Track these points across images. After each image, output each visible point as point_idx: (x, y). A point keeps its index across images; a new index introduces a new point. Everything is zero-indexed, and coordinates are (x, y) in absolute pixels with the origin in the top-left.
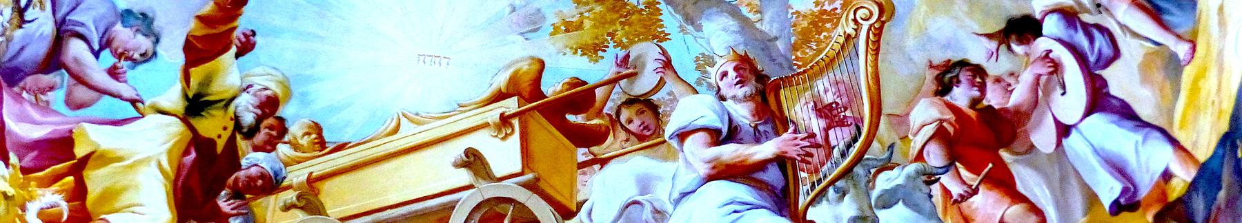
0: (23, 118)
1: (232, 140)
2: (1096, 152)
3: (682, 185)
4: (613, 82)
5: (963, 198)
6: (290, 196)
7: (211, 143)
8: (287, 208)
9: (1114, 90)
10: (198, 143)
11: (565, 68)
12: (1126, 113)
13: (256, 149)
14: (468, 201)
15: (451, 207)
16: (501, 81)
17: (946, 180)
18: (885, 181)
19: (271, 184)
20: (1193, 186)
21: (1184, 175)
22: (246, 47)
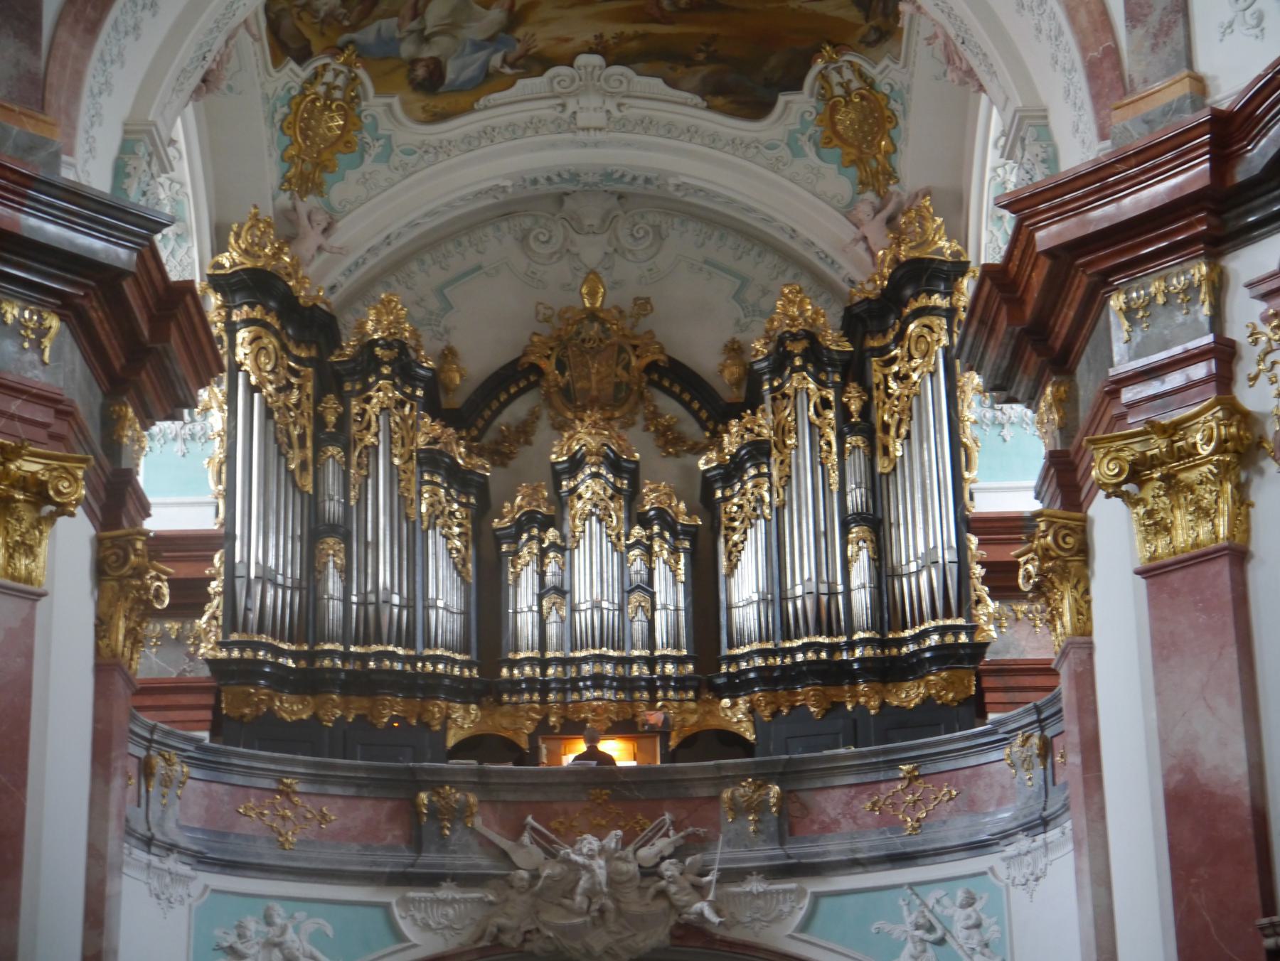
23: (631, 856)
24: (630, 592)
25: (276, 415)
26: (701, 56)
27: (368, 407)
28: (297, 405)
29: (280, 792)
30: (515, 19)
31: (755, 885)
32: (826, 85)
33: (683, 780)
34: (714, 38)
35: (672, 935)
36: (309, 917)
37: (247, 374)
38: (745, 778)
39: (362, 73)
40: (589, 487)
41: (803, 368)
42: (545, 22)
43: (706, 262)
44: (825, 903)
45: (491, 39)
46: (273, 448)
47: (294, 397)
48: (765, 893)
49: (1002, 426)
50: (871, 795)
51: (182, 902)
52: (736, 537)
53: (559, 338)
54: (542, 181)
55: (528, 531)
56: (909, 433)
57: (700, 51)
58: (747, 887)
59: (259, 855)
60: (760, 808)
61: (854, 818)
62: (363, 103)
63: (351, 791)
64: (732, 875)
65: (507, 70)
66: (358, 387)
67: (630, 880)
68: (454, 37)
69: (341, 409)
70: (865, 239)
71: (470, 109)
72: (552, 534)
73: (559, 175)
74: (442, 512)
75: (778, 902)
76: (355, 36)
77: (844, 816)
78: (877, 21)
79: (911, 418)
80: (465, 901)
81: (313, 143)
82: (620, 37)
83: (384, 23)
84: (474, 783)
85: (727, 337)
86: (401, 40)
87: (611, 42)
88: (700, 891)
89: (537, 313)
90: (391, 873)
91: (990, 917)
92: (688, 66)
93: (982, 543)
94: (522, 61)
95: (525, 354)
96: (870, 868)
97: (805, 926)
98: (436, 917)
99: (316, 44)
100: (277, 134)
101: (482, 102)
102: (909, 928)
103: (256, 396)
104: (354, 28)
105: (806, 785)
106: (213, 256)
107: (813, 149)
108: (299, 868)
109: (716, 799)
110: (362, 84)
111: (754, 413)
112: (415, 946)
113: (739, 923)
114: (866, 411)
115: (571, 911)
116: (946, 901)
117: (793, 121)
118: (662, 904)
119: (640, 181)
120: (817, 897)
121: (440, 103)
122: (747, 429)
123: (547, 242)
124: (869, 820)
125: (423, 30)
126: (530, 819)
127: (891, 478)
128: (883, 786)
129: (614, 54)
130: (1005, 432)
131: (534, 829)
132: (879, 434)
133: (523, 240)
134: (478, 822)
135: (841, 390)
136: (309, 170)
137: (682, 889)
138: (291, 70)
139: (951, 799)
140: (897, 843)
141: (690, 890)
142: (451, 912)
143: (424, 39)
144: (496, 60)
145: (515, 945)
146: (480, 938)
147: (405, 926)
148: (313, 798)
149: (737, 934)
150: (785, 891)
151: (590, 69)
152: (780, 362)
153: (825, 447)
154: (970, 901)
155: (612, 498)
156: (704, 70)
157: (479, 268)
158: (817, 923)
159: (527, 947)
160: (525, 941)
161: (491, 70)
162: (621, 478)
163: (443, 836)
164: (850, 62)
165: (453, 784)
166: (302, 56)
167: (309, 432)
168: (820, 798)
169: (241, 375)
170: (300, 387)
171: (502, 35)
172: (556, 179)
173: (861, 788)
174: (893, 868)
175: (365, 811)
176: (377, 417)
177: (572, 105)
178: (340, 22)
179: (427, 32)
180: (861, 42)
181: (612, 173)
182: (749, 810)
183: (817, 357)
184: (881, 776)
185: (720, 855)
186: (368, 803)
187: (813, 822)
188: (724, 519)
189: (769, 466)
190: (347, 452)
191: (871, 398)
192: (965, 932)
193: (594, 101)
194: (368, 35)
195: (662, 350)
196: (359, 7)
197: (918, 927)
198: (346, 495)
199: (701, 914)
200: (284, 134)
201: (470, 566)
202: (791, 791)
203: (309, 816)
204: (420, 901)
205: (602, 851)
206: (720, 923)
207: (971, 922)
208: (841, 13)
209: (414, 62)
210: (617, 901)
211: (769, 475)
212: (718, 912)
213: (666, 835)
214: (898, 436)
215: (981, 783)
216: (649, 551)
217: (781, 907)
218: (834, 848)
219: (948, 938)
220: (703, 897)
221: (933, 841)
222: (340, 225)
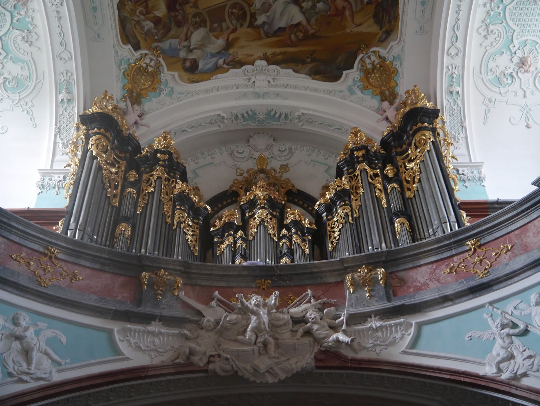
24: (281, 257)
25: (104, 172)
26: (309, 60)
27: (151, 178)
28: (117, 173)
29: (46, 255)
30: (229, 45)
31: (375, 323)
32: (363, 64)
33: (317, 273)
34: (314, 51)
35: (316, 359)
36: (48, 328)
37: (92, 152)
38: (360, 266)
39: (161, 59)
40: (260, 214)
41: (363, 161)
42: (242, 47)
43: (312, 160)
44: (426, 329)
45: (218, 53)
46: (99, 181)
47: (114, 170)
48: (381, 327)
49: (465, 181)
50: (448, 265)
52: (336, 234)
53: (246, 181)
54: (240, 116)
55: (228, 232)
56: (420, 181)
57: (308, 58)
61: (438, 280)
62: (162, 74)
63: (97, 266)
64: (356, 319)
65: (225, 66)
66: (147, 170)
67: (285, 324)
68: (203, 51)
69: (137, 176)
70: (387, 119)
71: (210, 79)
72: (240, 233)
73: (247, 113)
74: (184, 222)
75: (392, 332)
76: (160, 44)
77: (431, 280)
78: (386, 27)
79: (421, 172)
80: (168, 335)
81: (138, 85)
82: (274, 54)
83: (173, 41)
84: (180, 271)
85: (323, 184)
86: (180, 50)
87: (270, 56)
88: (334, 328)
89: (237, 172)
90: (116, 311)
92: (303, 64)
93: (467, 216)
94: (232, 63)
95: (231, 187)
96: (457, 301)
97: (414, 343)
98: (147, 341)
99: (142, 44)
100: (121, 74)
101: (214, 77)
103: (95, 161)
104: (160, 41)
105: (401, 268)
106: (84, 111)
107: (360, 91)
108: (47, 294)
109: (342, 282)
110: (162, 66)
111: (341, 179)
112: (127, 359)
113: (365, 348)
114: (397, 174)
115: (243, 343)
117: (350, 82)
118: (307, 340)
119: (283, 117)
120: (420, 326)
121: (196, 77)
122: (338, 186)
123: (243, 152)
124: (449, 279)
125: (190, 46)
126: (217, 293)
127: (414, 200)
128: (455, 258)
129: (271, 61)
130: (466, 184)
131: (219, 300)
132: (405, 183)
133: (232, 154)
134: (182, 294)
135: (383, 169)
136: (135, 97)
137: (323, 327)
138: (129, 49)
139: (508, 251)
141: (327, 328)
142: (157, 340)
143: (190, 51)
144: (221, 62)
145: (202, 365)
146: (178, 358)
147: (122, 346)
148: (69, 265)
149: (363, 355)
150: (396, 325)
151: (261, 67)
152: (351, 161)
153: (378, 191)
155: (271, 219)
156: (310, 66)
157: (212, 163)
158: (423, 341)
159: (211, 366)
160: (209, 362)
161: (218, 65)
162: (276, 212)
163: (157, 299)
164: (374, 52)
165: (166, 269)
166: (137, 48)
167: (120, 184)
168: (412, 274)
169: (89, 153)
170: (118, 168)
171: (223, 51)
172: (246, 115)
173: (440, 263)
175: (105, 279)
176: (155, 181)
177: (253, 79)
178: (154, 36)
179: (191, 47)
180: (378, 41)
181: (271, 111)
183: (369, 158)
184: (454, 252)
186: (108, 275)
187: (409, 287)
188: (329, 228)
189: (350, 202)
190: (138, 193)
191: (398, 170)
193: (263, 77)
194: (166, 45)
195: (293, 186)
196: (162, 31)
197: (503, 326)
198: (136, 210)
200: (126, 78)
201: (197, 248)
202: (391, 273)
203: (64, 273)
204: (135, 331)
208: (369, 30)
209: (185, 60)
210: (276, 339)
211: (351, 206)
213: (309, 302)
214: (414, 183)
215: (530, 234)
216: (290, 240)
217: (394, 335)
222: (147, 116)
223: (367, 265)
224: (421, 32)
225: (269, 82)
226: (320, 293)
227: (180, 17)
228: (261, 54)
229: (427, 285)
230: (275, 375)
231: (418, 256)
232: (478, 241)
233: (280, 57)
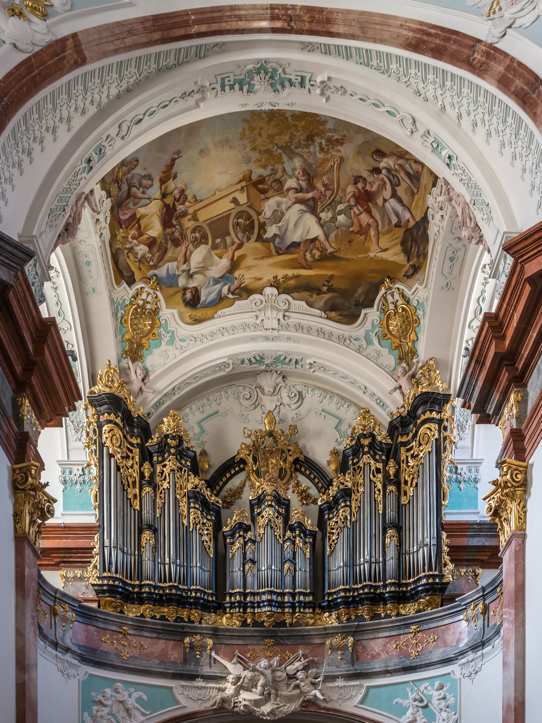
0: (125, 214)
1: (174, 203)
2: (392, 208)
3: (288, 205)
4: (270, 175)
5: (359, 215)
6: (190, 217)
7: (169, 205)
8: (189, 220)
9: (398, 194)
10: (166, 206)
11: (258, 172)
12: (400, 201)
13: (180, 205)
14: (234, 212)
15: (230, 215)
16: (241, 177)
17: (355, 209)
18: (340, 207)
19: (184, 214)
20: (414, 226)
21: (412, 223)
22: (175, 177)
23: (283, 669)
29: (121, 633)
38: (337, 634)
51: (75, 677)
58: (336, 684)
59: (112, 661)
60: (345, 647)
61: (387, 652)
67: (283, 680)
77: (383, 651)
91: (450, 694)
102: (411, 701)
105: (365, 637)
109: (324, 644)
116: (429, 688)
118: (297, 691)
124: (394, 653)
128: (402, 637)
140: (407, 663)
141: (310, 685)
154: (441, 687)
168: (372, 643)
174: (405, 674)
182: (338, 649)
184: (402, 632)
185: (325, 670)
187: (368, 654)
192: (438, 702)
197: (415, 700)
199: (315, 696)
205: (270, 666)
206: (324, 699)
207: (440, 697)
212: (323, 695)
213: (300, 660)
218: (377, 666)
219: (429, 705)
220: (316, 689)
221: (424, 660)
223: (342, 633)
224: (447, 289)
225: (279, 320)
226: (308, 651)
227: (177, 234)
228: (271, 277)
229: (380, 654)
230: (275, 715)
231: (378, 630)
232: (418, 627)
233: (292, 282)
